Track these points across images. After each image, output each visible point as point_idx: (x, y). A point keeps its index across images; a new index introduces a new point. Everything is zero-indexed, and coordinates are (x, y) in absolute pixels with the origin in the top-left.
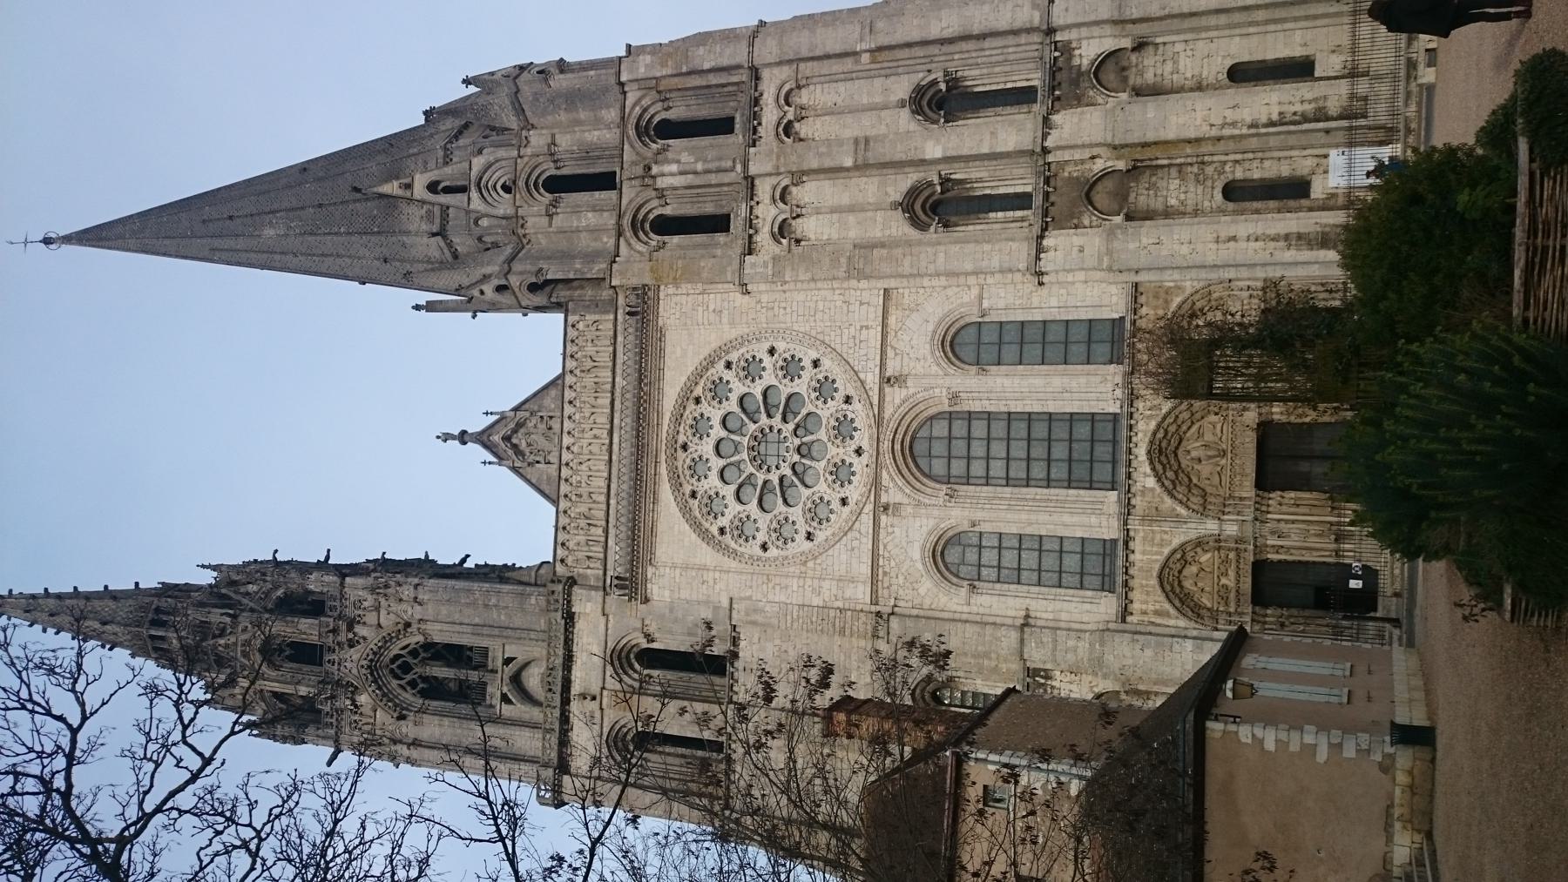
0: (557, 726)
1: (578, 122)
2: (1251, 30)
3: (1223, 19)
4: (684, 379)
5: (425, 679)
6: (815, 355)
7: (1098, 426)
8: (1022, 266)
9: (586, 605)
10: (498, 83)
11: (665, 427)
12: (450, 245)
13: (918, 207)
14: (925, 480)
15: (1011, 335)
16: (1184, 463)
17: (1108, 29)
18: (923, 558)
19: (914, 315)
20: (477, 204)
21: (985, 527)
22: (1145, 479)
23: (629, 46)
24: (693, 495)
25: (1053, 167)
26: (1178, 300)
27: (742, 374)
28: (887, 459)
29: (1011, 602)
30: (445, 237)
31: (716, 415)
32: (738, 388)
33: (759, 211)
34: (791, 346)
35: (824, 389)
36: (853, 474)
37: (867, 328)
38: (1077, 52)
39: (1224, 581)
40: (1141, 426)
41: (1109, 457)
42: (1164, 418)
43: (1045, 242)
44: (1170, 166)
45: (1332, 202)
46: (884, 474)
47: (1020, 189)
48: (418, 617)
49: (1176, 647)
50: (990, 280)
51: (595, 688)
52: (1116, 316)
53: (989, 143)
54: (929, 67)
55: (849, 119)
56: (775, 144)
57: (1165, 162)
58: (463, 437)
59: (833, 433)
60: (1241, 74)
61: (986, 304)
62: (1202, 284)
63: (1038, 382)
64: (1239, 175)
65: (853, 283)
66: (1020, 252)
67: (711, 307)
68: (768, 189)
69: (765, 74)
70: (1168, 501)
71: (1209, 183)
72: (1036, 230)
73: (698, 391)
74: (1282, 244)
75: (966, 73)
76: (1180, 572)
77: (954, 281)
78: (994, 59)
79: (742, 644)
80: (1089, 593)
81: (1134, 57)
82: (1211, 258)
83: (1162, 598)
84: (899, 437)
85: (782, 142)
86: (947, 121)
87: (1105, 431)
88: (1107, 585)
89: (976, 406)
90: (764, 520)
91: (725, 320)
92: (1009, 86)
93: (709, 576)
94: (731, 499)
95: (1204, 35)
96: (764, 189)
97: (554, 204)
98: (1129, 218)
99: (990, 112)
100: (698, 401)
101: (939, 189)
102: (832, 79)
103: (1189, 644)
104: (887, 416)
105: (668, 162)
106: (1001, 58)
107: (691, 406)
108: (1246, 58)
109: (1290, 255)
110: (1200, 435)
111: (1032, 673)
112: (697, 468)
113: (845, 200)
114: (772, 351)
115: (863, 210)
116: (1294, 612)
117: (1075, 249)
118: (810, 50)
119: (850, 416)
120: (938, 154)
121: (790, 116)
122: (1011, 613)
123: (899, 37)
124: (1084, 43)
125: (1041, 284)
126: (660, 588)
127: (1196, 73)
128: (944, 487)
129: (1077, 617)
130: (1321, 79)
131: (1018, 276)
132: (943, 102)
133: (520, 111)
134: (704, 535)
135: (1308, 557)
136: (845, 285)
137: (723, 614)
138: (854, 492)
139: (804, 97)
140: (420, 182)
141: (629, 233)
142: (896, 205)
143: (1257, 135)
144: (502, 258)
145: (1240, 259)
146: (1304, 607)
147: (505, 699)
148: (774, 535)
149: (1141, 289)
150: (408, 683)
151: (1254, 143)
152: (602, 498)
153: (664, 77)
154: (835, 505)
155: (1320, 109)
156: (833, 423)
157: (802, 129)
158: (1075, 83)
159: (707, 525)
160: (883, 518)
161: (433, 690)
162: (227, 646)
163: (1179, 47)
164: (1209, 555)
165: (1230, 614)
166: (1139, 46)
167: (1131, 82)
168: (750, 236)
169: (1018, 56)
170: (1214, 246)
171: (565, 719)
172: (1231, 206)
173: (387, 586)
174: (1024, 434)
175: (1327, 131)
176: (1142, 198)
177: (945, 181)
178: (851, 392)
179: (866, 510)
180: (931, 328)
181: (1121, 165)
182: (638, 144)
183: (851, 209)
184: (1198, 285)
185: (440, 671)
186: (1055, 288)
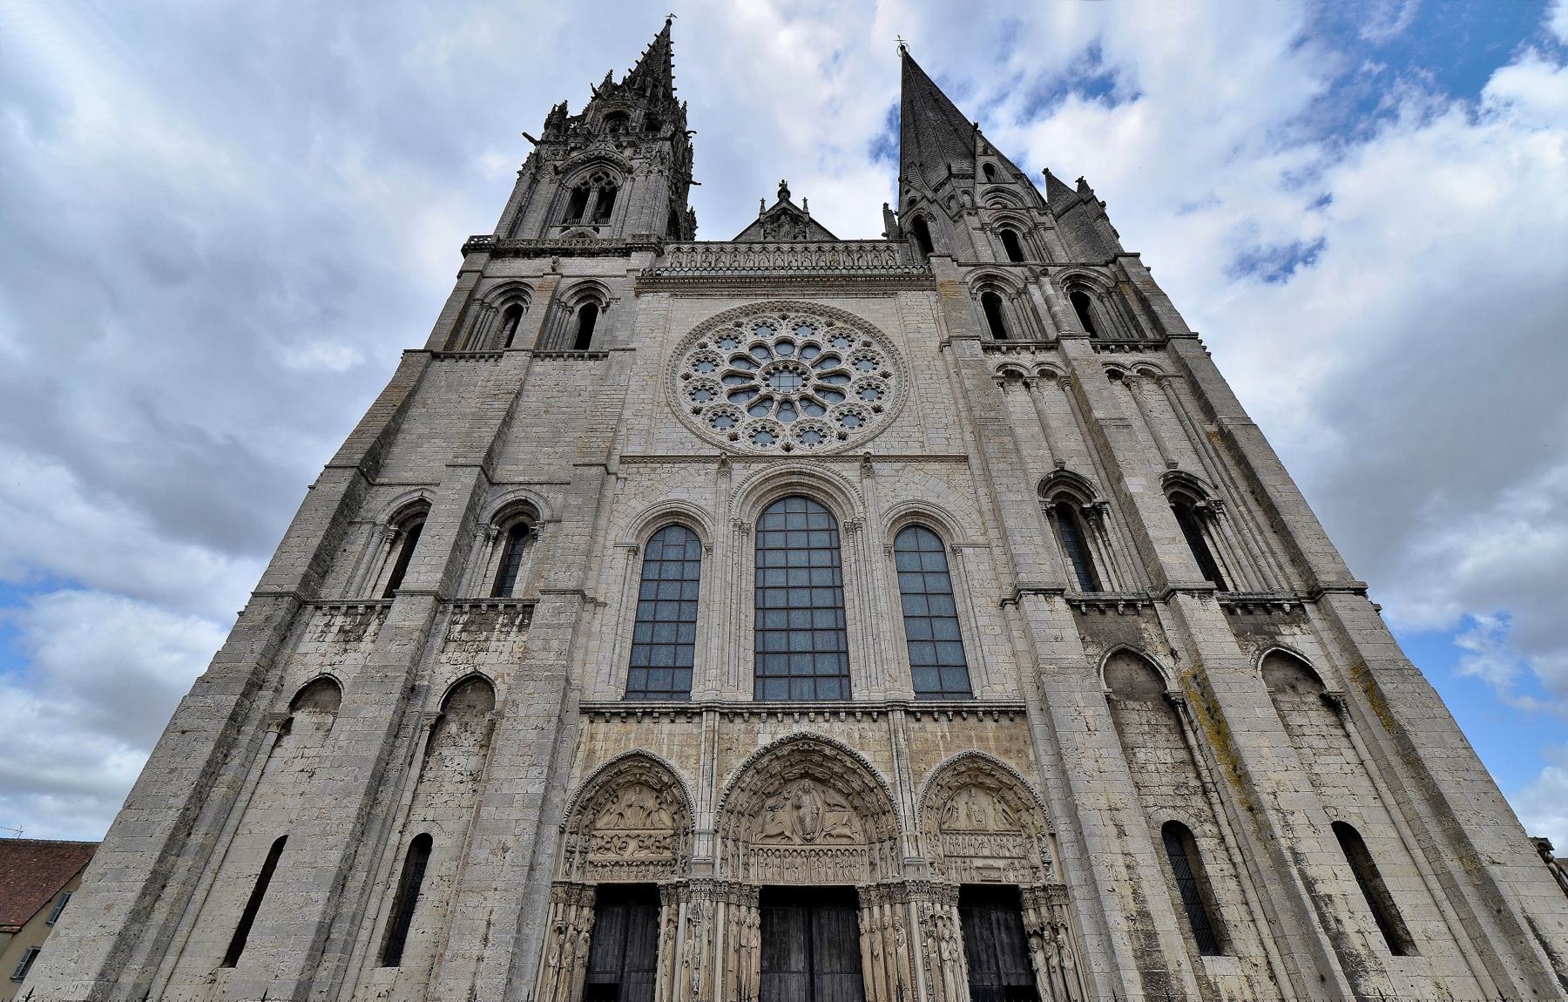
6: (887, 406)
8: (1023, 577)
12: (942, 184)
13: (1061, 489)
14: (759, 508)
16: (794, 788)
17: (1342, 662)
18: (669, 502)
19: (943, 485)
21: (705, 565)
22: (767, 734)
24: (739, 325)
25: (1148, 611)
26: (1011, 764)
27: (860, 355)
29: (616, 588)
30: (949, 178)
34: (893, 389)
38: (1296, 630)
39: (633, 845)
42: (851, 755)
43: (1057, 598)
44: (1189, 748)
49: (535, 772)
52: (977, 693)
54: (1221, 485)
57: (1192, 741)
60: (1347, 835)
61: (966, 551)
63: (883, 606)
64: (1204, 844)
65: (968, 428)
68: (1050, 360)
69: (1161, 354)
70: (738, 763)
71: (1179, 802)
73: (839, 324)
74: (1133, 907)
75: (1223, 522)
76: (646, 784)
77: (988, 516)
78: (1252, 544)
79: (591, 363)
80: (624, 674)
81: (1312, 698)
82: (1084, 800)
83: (610, 758)
84: (806, 480)
88: (630, 692)
93: (658, 334)
95: (1382, 786)
103: (537, 789)
106: (1256, 551)
107: (823, 320)
111: (529, 608)
114: (885, 375)
117: (1056, 632)
119: (826, 441)
122: (602, 589)
125: (1003, 604)
126: (655, 303)
129: (592, 657)
131: (1006, 580)
135: (662, 968)
136: (965, 421)
139: (1148, 387)
141: (980, 272)
142: (1060, 465)
145: (1093, 844)
146: (589, 968)
148: (699, 385)
149: (1018, 720)
158: (1258, 630)
160: (716, 466)
161: (579, 197)
163: (1349, 755)
164: (669, 823)
165: (584, 852)
166: (1332, 704)
168: (999, 349)
169: (1266, 569)
170: (1103, 803)
171: (539, 253)
172: (1158, 833)
174: (818, 603)
177: (1098, 511)
178: (851, 439)
180: (931, 500)
181: (1173, 686)
182: (1063, 275)
183: (1044, 427)
184: (1037, 790)
185: (593, 197)
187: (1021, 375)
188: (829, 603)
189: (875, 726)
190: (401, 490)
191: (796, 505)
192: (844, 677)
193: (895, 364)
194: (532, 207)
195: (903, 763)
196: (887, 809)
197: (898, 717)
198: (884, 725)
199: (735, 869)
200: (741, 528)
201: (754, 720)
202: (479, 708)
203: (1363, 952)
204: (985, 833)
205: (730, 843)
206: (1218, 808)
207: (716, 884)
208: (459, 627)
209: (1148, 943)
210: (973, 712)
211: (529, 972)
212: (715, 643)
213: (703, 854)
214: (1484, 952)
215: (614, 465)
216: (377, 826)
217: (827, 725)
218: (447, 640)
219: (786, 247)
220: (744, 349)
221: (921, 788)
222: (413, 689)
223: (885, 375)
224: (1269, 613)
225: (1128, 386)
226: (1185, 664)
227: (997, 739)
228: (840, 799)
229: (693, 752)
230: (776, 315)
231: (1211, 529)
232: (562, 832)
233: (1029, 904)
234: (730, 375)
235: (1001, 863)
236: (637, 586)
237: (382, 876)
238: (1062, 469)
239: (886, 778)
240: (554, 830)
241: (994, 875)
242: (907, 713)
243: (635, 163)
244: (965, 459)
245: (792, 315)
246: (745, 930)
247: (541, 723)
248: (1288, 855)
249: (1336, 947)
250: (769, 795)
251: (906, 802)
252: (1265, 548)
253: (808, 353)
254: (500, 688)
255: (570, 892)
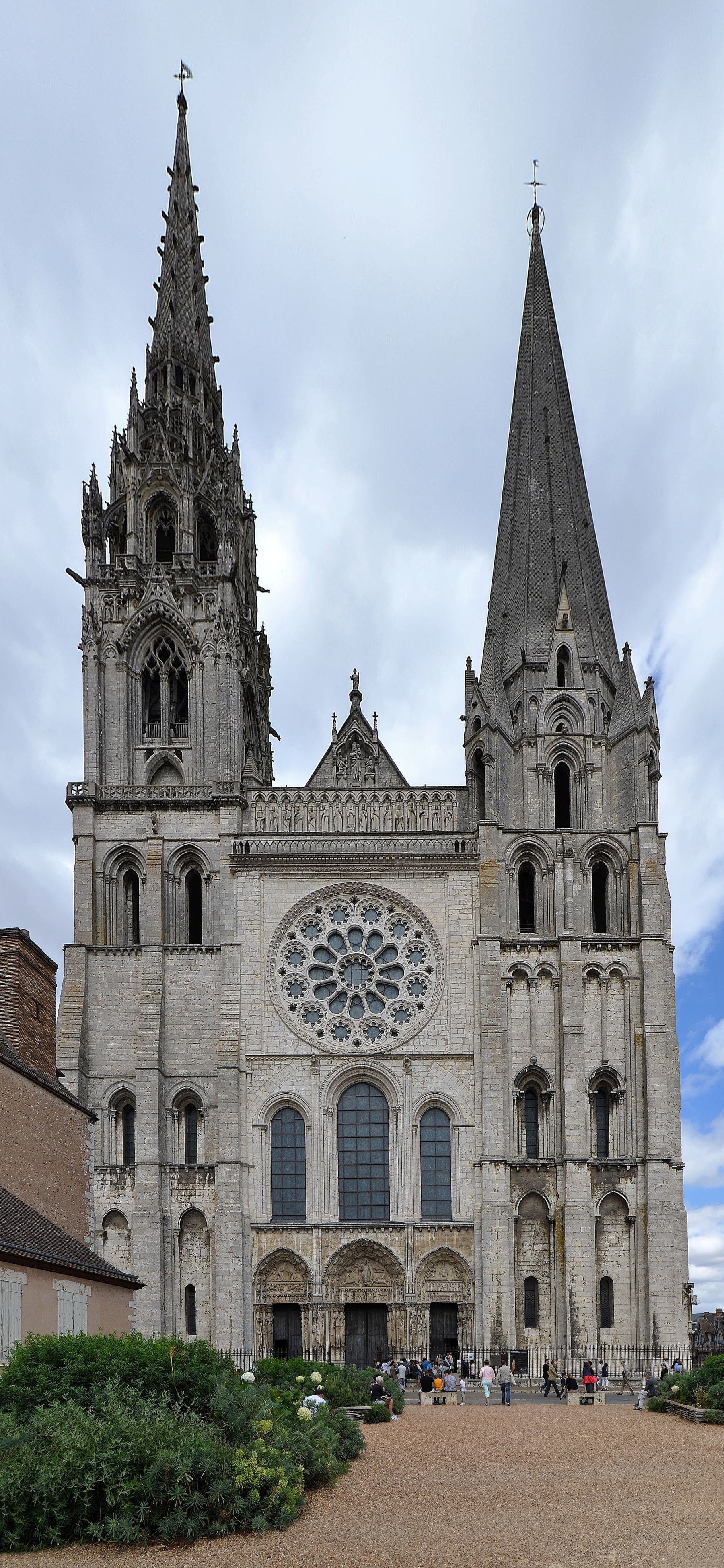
0: (128, 797)
1: (610, 793)
2: (633, 1290)
3: (641, 1272)
4: (407, 896)
5: (157, 675)
6: (426, 1005)
7: (381, 1209)
8: (486, 1152)
9: (227, 819)
10: (646, 712)
11: (368, 882)
15: (441, 1149)
17: (641, 1201)
19: (455, 1079)
20: (548, 697)
22: (346, 1239)
23: (664, 836)
24: (319, 911)
26: (462, 1253)
27: (412, 946)
28: (351, 1064)
30: (522, 668)
31: (380, 926)
32: (401, 944)
33: (534, 954)
34: (433, 986)
35: (402, 1013)
36: (341, 1040)
37: (447, 1044)
38: (629, 1181)
39: (286, 1288)
40: (380, 1235)
41: (361, 1217)
42: (386, 1248)
43: (502, 1166)
44: (549, 1244)
45: (522, 1340)
46: (341, 1062)
47: (540, 1149)
48: (205, 661)
50: (478, 1131)
51: (162, 833)
52: (453, 1216)
53: (573, 1122)
54: (629, 1079)
55: (597, 1022)
56: (583, 963)
58: (356, 696)
59: (370, 1022)
60: (606, 1285)
61: (461, 1129)
62: (472, 1267)
63: (408, 1167)
64: (541, 1286)
66: (495, 1151)
67: (462, 916)
69: (634, 953)
71: (537, 1268)
72: (511, 1160)
73: (398, 910)
74: (495, 1312)
75: (621, 1107)
77: (478, 1106)
79: (208, 956)
80: (270, 1207)
82: (487, 1270)
83: (270, 1251)
85: (584, 969)
86: (590, 1095)
87: (379, 1212)
88: (275, 1216)
89: (392, 1126)
90: (302, 970)
91: (452, 929)
92: (611, 1138)
94: (316, 942)
95: (633, 1261)
96: (548, 956)
97: (546, 773)
98: (516, 1220)
99: (594, 1126)
100: (391, 910)
101: (544, 1092)
102: (626, 1007)
104: (382, 1062)
105: (574, 873)
106: (630, 1130)
108: (615, 1287)
109: (488, 1318)
110: (377, 1271)
111: (212, 1170)
112: (339, 913)
113: (539, 1022)
115: (531, 1036)
116: (270, 1328)
118: (648, 986)
120: (567, 1088)
121: (603, 975)
122: (250, 1156)
123: (651, 1054)
124: (634, 1185)
126: (247, 884)
127: (609, 1258)
128: (335, 1107)
130: (599, 1331)
131: (479, 1150)
132: (604, 1091)
133: (622, 737)
134: (287, 921)
136: (477, 1025)
137: (228, 939)
138: (328, 1042)
139: (615, 985)
140: (568, 639)
142: (533, 1061)
143: (565, 1295)
144: (503, 725)
147: (149, 752)
148: (292, 979)
149: (470, 1231)
150: (152, 658)
151: (560, 1294)
152: (312, 830)
153: (639, 867)
154: (317, 1027)
155: (579, 1331)
156: (378, 1021)
157: (592, 986)
158: (608, 1181)
159: (296, 923)
160: (309, 1063)
162: (161, 453)
164: (301, 1278)
166: (629, 1222)
167: (605, 1217)
168: (515, 946)
170: (495, 1272)
171: (135, 806)
172: (522, 1282)
173: (228, 626)
174: (375, 1161)
175: (565, 1336)
176: (530, 1228)
177: (548, 1097)
178: (400, 1035)
179: (314, 1050)
180: (446, 1091)
181: (551, 1213)
182: (589, 847)
183: (532, 1027)
184: (471, 1265)
186: (471, 1175)
187: (526, 974)
188: (380, 1161)
189: (398, 1234)
190: (108, 1082)
191: (363, 1091)
192: (386, 1206)
193: (437, 959)
194: (109, 715)
195: (410, 1252)
196: (401, 1273)
197: (410, 1230)
198: (403, 1234)
199: (333, 1298)
200: (328, 1111)
201: (339, 1232)
202: (199, 1225)
203: (582, 1327)
204: (446, 1281)
205: (330, 1288)
206: (552, 1271)
207: (324, 1304)
208: (176, 1181)
209: (498, 1323)
210: (447, 1227)
211: (251, 1337)
212: (316, 1190)
213: (317, 1293)
214: (637, 1327)
215: (243, 1065)
216: (169, 1283)
217: (375, 1234)
218: (172, 1189)
219: (356, 795)
220: (323, 940)
221: (418, 1264)
222: (164, 1218)
223: (429, 970)
224: (618, 1171)
225: (600, 985)
226: (560, 1203)
227: (458, 1240)
228: (381, 1267)
229: (310, 1248)
230: (348, 898)
231: (615, 1110)
232: (253, 1284)
233: (460, 1310)
234: (314, 969)
235: (451, 1294)
236: (269, 1152)
237: (178, 1302)
238: (534, 1065)
239: (401, 1259)
240: (250, 1284)
241: (447, 1299)
242: (415, 1228)
243: (198, 631)
244: (472, 1057)
245: (361, 898)
246: (338, 1321)
247: (234, 1236)
248: (568, 1292)
249: (572, 1326)
250: (347, 1266)
251: (410, 1270)
252: (634, 1129)
253: (374, 941)
254: (208, 1216)
255: (262, 1308)
